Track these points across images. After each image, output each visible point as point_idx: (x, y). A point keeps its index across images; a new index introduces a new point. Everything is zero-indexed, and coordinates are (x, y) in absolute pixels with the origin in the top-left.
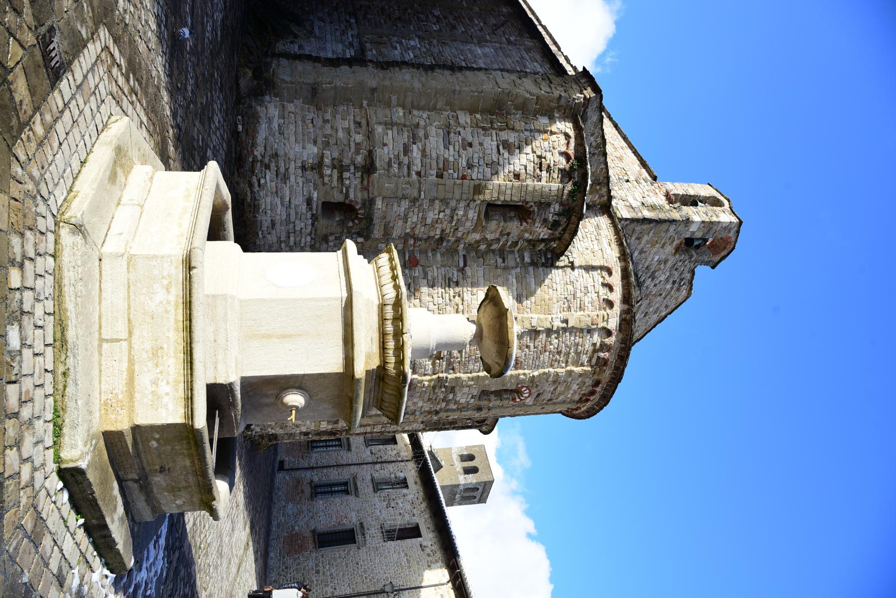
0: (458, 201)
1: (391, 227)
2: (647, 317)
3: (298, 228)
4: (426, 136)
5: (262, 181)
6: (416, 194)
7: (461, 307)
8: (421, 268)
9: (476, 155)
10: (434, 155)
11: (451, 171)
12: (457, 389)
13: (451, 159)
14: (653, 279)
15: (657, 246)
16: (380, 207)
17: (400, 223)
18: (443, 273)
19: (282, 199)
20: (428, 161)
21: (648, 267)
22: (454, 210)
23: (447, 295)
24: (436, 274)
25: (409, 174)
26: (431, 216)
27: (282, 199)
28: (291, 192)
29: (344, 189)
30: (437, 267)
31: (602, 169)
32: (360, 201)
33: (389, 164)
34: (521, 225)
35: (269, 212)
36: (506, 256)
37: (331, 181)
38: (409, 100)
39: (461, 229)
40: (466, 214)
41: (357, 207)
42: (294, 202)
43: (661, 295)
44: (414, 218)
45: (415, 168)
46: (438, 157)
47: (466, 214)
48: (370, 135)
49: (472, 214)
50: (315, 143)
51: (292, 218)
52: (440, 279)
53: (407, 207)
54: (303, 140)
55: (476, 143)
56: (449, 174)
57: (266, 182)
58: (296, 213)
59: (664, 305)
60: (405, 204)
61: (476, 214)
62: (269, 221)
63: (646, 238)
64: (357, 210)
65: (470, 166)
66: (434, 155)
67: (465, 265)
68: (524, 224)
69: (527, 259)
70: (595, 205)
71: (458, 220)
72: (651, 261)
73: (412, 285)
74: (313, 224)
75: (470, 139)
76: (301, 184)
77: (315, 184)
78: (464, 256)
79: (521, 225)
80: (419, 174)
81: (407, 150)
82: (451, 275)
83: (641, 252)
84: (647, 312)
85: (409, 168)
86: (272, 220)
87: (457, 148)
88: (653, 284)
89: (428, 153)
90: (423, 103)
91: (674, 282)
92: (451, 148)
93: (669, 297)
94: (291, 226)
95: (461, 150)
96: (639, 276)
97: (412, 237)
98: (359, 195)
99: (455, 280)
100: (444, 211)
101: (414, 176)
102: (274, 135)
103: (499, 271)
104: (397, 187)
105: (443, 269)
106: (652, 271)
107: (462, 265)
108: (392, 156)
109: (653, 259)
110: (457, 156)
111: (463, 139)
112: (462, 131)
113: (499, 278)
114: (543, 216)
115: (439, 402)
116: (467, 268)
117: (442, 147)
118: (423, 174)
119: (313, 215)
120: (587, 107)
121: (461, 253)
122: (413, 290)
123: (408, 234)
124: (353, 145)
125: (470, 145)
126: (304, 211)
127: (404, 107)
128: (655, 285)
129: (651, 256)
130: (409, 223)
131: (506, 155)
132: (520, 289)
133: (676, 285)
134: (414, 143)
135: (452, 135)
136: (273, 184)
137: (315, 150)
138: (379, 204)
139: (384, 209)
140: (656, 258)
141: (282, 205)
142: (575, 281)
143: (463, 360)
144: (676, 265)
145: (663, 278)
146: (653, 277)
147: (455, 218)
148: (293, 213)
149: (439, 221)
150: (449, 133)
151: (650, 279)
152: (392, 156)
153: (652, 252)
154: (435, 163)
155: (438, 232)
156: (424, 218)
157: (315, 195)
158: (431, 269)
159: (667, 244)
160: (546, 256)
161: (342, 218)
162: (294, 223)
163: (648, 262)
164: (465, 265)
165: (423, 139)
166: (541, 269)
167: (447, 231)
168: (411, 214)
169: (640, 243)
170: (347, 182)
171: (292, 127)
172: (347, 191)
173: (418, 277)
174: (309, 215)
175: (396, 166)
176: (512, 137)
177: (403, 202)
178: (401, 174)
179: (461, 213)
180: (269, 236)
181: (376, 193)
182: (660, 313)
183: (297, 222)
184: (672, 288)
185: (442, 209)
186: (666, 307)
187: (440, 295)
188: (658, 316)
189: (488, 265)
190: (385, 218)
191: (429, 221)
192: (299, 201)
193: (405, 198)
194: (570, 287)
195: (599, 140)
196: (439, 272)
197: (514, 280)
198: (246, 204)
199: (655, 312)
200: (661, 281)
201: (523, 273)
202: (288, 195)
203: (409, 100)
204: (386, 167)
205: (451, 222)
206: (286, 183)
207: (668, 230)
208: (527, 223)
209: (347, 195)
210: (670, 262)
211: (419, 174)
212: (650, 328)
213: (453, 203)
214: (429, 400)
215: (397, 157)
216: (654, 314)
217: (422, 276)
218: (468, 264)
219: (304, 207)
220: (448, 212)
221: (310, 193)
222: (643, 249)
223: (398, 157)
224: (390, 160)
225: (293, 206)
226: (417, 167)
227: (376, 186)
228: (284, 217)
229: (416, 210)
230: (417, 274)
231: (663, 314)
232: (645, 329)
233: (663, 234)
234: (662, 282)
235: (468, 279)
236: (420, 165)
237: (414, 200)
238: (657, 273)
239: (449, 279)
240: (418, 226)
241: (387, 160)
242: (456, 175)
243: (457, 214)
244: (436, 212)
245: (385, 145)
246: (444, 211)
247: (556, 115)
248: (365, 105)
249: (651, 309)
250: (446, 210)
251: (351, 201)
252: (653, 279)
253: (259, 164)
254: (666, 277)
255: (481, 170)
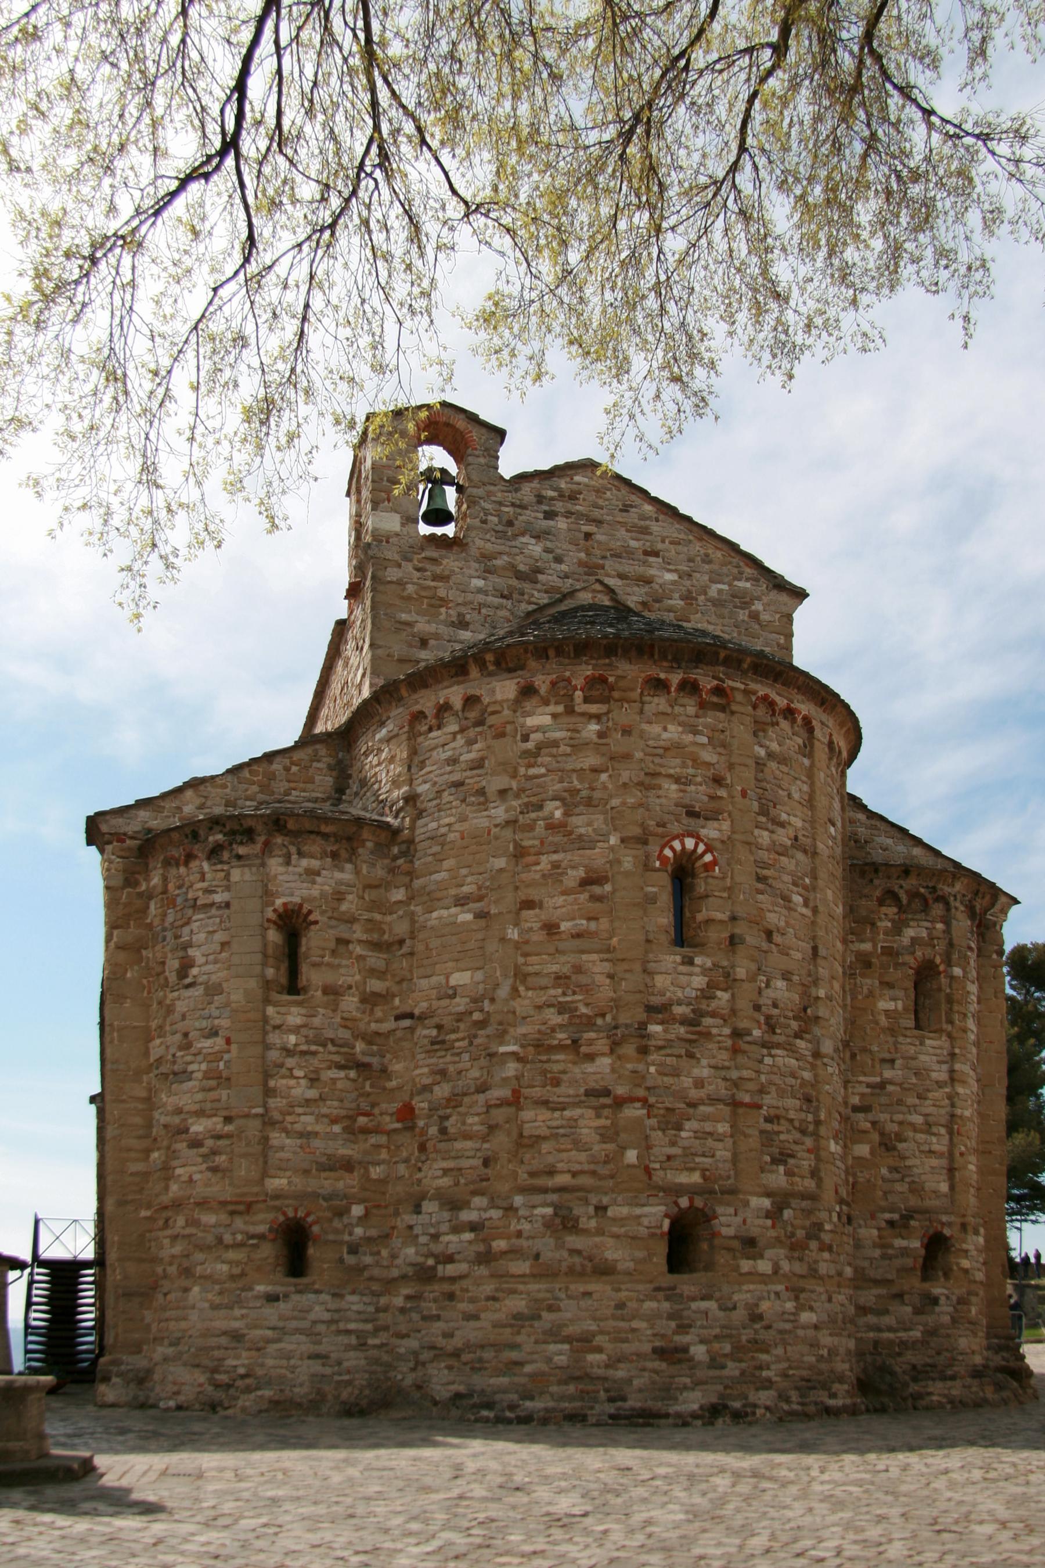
0: (267, 1047)
1: (329, 1159)
2: (660, 546)
3: (327, 1316)
4: (179, 1111)
5: (242, 1371)
6: (257, 1123)
7: (477, 1016)
8: (417, 1099)
9: (197, 1024)
10: (199, 1096)
11: (222, 1065)
12: (656, 1000)
13: (204, 1066)
14: (538, 571)
15: (442, 593)
16: (284, 1181)
17: (316, 1143)
18: (423, 1055)
19: (269, 1341)
20: (209, 1105)
21: (503, 596)
22: (289, 1052)
23: (457, 1044)
24: (426, 1070)
25: (228, 1136)
26: (301, 1090)
27: (269, 1341)
28: (256, 1327)
29: (251, 1242)
30: (417, 1067)
31: (250, 772)
32: (271, 1216)
33: (214, 1170)
34: (316, 922)
35: (292, 1362)
36: (397, 938)
37: (238, 1263)
38: (134, 1143)
39: (329, 1034)
40: (296, 1030)
41: (281, 1218)
42: (274, 1321)
43: (588, 536)
44: (307, 1121)
45: (219, 1127)
46: (203, 1090)
47: (296, 1030)
48: (177, 1205)
49: (295, 1017)
50: (186, 1290)
51: (305, 1324)
52: (433, 1060)
53: (284, 1135)
54: (185, 1308)
55: (181, 1026)
56: (227, 1067)
57: (243, 1365)
58: (295, 1318)
59: (620, 517)
60: (277, 1138)
61: (293, 1009)
62: (311, 1362)
63: (423, 626)
64: (288, 1219)
65: (214, 1033)
66: (199, 1096)
67: (410, 1016)
68: (312, 918)
69: (398, 895)
70: (340, 762)
71: (308, 1042)
72: (486, 593)
73: (441, 1113)
74: (318, 1292)
75: (178, 1037)
76: (244, 1311)
77: (243, 1290)
78: (398, 1018)
79: (316, 922)
80: (228, 1120)
81: (196, 1143)
82: (426, 1041)
83: (462, 624)
84: (646, 553)
85: (219, 1137)
86: (309, 1358)
87: (189, 1058)
88: (554, 565)
89: (197, 1107)
90: (138, 1120)
91: (550, 515)
92: (191, 1068)
93: (596, 513)
94: (321, 1328)
95: (193, 1050)
96: (531, 607)
97: (352, 1118)
98: (261, 1216)
99: (434, 1032)
100: (291, 1070)
101: (229, 1128)
102: (181, 1353)
103: (420, 947)
104: (245, 1155)
105: (419, 1057)
106: (514, 582)
107: (407, 1023)
108: (204, 1166)
109: (480, 591)
110: (200, 1058)
111: (181, 1048)
112: (172, 1050)
113: (431, 946)
114: (292, 885)
115: (699, 1033)
116: (417, 1012)
117: (191, 1084)
118: (226, 1113)
119: (300, 1292)
120: (125, 834)
121: (389, 1025)
122: (448, 1111)
123: (345, 1129)
124: (188, 1231)
125: (186, 1035)
126: (290, 1305)
127: (148, 1152)
128: (558, 560)
129: (470, 597)
130: (318, 1128)
131: (195, 971)
132: (446, 902)
133: (559, 506)
134: (186, 1130)
135: (176, 1068)
136: (244, 1354)
137: (196, 1289)
138: (277, 1183)
139: (288, 1173)
140: (480, 583)
141: (279, 1340)
142: (436, 789)
143: (580, 997)
144: (500, 528)
145: (536, 549)
146: (531, 575)
147: (304, 1048)
148: (294, 1324)
149: (312, 1076)
150: (175, 1074)
151: (540, 577)
152: (204, 1166)
153: (460, 600)
154: (212, 1093)
155: (342, 1074)
156: (308, 1102)
157: (261, 1288)
158: (417, 1080)
159: (438, 570)
160: (395, 858)
161: (310, 1243)
162: (315, 1322)
163: (490, 599)
164: (410, 1016)
165: (183, 1116)
166: (417, 863)
167: (337, 1058)
168: (298, 1127)
169: (437, 636)
170: (239, 1237)
171: (172, 1324)
172: (253, 1237)
173: (430, 1102)
174: (296, 1297)
175: (217, 1158)
176: (173, 964)
177: (274, 1142)
178: (228, 1149)
179: (292, 1039)
180: (346, 1364)
181: (255, 1189)
182: (649, 518)
183: (312, 1316)
184: (568, 514)
185: (288, 1073)
186: (625, 509)
187: (457, 1059)
188: (657, 520)
189: (411, 971)
190: (306, 1172)
191: (312, 1094)
192: (271, 1313)
193: (267, 1139)
194: (446, 797)
195: (189, 793)
196: (421, 1063)
197: (435, 915)
198: (276, 1398)
199: (645, 531)
200: (547, 550)
201: (425, 898)
202: (259, 1332)
203: (134, 1143)
204: (220, 1175)
205: (314, 1053)
206: (244, 1335)
207: (401, 583)
208: (310, 912)
209: (261, 1237)
210: (489, 546)
211: (228, 1120)
212: (695, 529)
213: (274, 1055)
214: (691, 1055)
215: (204, 1156)
216: (651, 534)
217: (427, 1095)
218: (408, 1010)
219: (282, 1305)
220: (290, 1062)
221: (257, 1297)
222: (453, 624)
223: (204, 1156)
224: (209, 1169)
225: (281, 1324)
226: (216, 1123)
227: (245, 1190)
228: (303, 1338)
229: (289, 1118)
230: (425, 1105)
231: (648, 508)
232: (700, 539)
233: (411, 589)
234: (549, 544)
235: (434, 1007)
236: (214, 1119)
237: (268, 1122)
238: (522, 567)
239: (433, 1043)
240: (325, 1110)
241: (209, 1174)
242: (226, 1057)
243: (296, 1045)
244: (292, 1082)
245: (191, 1180)
246: (291, 1070)
247: (144, 887)
248: (148, 1213)
249: (633, 544)
250: (289, 1066)
251: (271, 1230)
252: (538, 571)
253: (217, 1376)
254: (533, 541)
255: (216, 1013)
